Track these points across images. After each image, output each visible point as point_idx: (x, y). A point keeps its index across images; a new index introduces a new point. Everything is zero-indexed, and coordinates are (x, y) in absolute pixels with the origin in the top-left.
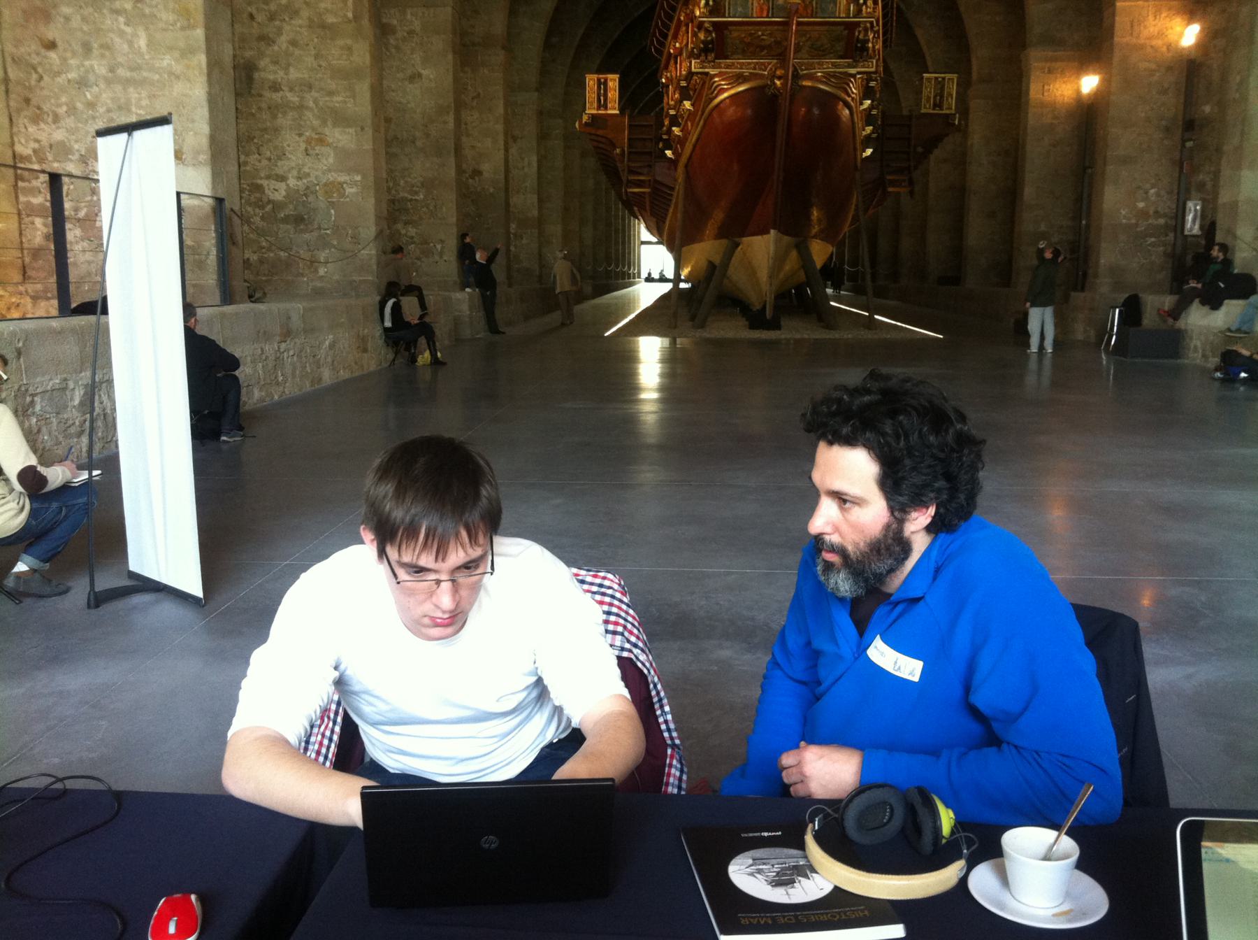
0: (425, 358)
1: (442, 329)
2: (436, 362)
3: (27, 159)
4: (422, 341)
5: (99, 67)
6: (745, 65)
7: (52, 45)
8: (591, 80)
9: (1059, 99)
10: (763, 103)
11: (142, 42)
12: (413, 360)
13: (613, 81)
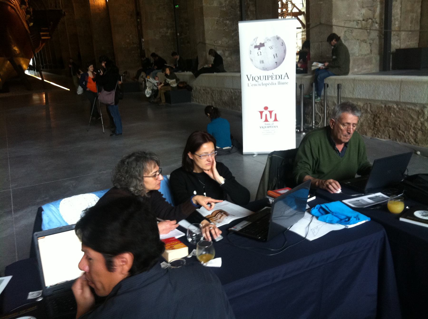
9: (100, 4)
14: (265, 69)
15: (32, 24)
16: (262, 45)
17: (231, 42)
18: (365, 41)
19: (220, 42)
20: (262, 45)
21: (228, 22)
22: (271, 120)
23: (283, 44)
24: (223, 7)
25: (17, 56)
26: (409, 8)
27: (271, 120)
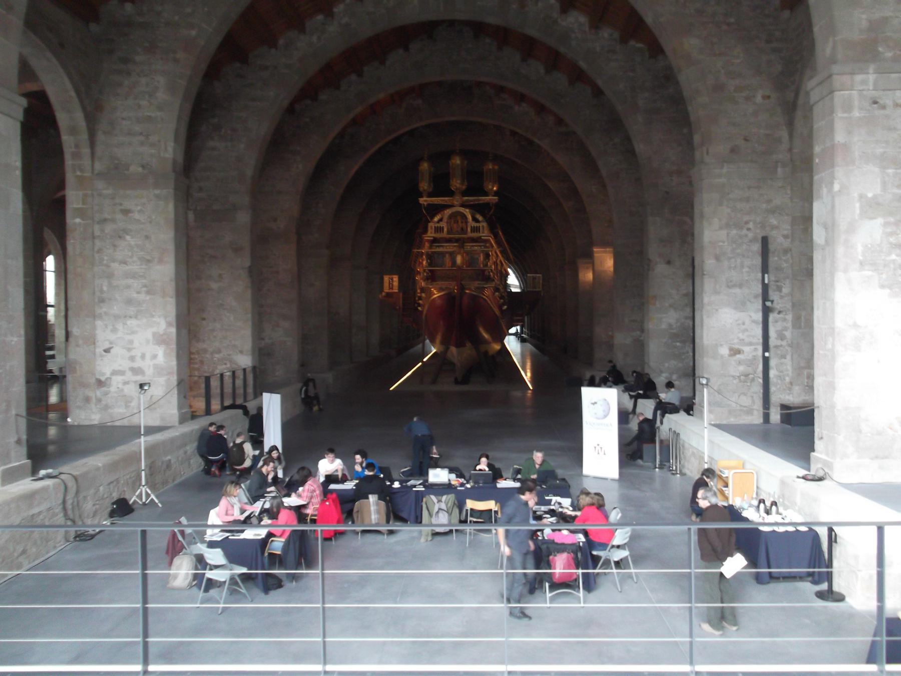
0: (316, 408)
1: (322, 397)
2: (320, 410)
3: (193, 353)
4: (315, 402)
5: (218, 326)
7: (204, 319)
8: (386, 279)
10: (450, 299)
11: (232, 318)
12: (311, 409)
13: (396, 279)
15: (505, 307)
16: (596, 403)
17: (680, 365)
18: (745, 394)
19: (667, 365)
20: (596, 403)
21: (678, 344)
22: (602, 453)
25: (486, 342)
26: (802, 365)
27: (602, 453)
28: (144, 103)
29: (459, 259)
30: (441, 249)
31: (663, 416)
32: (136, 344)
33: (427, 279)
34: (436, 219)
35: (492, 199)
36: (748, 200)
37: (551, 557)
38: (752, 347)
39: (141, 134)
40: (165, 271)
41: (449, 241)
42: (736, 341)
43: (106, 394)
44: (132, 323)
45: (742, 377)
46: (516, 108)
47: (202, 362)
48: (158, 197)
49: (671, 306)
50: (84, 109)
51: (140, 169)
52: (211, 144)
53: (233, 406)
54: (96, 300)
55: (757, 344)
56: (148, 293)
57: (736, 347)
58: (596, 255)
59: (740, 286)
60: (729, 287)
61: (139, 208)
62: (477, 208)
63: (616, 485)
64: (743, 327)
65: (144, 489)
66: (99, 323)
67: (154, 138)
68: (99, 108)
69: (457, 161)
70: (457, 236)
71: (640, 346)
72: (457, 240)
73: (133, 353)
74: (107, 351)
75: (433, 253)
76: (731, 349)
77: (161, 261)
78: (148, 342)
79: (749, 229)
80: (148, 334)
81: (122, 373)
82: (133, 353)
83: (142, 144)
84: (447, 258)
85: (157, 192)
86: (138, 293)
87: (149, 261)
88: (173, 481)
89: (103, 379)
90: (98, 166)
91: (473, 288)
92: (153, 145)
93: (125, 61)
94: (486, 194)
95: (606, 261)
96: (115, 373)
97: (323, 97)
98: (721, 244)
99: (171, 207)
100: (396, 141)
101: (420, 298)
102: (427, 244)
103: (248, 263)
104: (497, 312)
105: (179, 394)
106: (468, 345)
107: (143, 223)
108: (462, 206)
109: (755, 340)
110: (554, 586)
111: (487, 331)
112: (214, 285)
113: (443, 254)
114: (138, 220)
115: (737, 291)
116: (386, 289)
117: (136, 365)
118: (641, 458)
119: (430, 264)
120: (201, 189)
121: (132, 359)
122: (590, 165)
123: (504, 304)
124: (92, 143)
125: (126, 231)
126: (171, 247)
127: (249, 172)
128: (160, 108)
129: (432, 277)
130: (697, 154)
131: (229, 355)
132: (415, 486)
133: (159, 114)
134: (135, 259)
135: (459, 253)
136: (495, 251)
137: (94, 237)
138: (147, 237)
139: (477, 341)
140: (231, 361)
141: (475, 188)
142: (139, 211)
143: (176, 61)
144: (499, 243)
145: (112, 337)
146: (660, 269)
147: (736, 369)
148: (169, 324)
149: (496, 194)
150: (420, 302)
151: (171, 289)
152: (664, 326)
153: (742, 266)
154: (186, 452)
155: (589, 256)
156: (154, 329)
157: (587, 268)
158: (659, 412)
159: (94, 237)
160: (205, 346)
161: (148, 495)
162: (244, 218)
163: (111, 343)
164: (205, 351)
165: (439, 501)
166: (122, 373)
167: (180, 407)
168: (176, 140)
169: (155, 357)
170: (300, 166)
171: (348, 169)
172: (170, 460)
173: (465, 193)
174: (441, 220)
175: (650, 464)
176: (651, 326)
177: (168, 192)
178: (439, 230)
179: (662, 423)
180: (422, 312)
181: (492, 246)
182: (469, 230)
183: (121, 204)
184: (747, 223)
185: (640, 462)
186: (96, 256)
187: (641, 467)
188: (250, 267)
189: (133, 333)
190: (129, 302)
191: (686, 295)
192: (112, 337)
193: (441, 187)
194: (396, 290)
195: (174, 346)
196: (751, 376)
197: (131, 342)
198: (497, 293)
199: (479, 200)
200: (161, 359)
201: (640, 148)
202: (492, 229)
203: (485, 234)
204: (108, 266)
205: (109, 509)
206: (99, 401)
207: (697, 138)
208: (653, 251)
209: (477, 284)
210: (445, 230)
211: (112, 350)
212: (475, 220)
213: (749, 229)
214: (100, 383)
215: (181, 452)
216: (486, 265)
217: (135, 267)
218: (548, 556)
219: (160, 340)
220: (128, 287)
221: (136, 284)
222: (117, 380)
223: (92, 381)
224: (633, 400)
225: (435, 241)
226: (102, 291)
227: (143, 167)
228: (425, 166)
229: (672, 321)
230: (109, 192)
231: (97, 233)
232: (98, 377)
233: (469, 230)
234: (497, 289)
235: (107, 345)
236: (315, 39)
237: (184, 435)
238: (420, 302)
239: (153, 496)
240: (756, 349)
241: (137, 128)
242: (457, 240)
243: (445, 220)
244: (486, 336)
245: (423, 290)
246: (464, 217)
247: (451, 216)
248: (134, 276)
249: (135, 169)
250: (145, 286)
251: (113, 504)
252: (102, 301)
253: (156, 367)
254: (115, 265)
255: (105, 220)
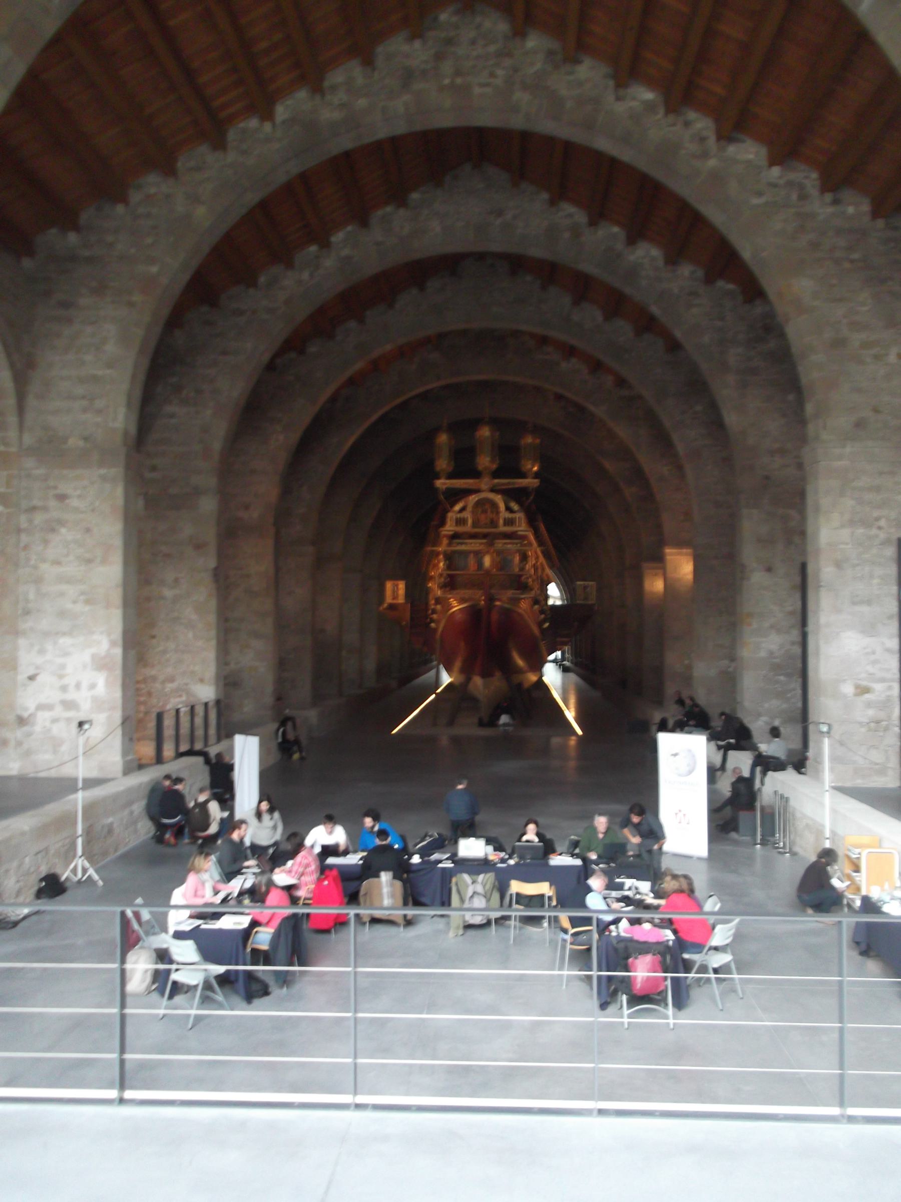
0: (296, 756)
2: (302, 759)
4: (295, 748)
5: (171, 645)
6: (467, 593)
7: (154, 637)
8: (389, 585)
10: (475, 614)
11: (190, 635)
12: (291, 756)
13: (402, 585)
14: (680, 775)
15: (547, 625)
17: (784, 706)
19: (766, 705)
20: (675, 755)
21: (782, 678)
23: (693, 756)
24: (775, 658)
25: (520, 671)
28: (89, 358)
29: (487, 561)
30: (463, 548)
31: (764, 773)
32: (69, 670)
33: (443, 586)
34: (457, 507)
35: (530, 482)
36: (877, 489)
37: (630, 960)
38: (886, 684)
39: (84, 397)
40: (111, 573)
41: (474, 536)
42: (863, 675)
43: (29, 735)
44: (65, 641)
45: (872, 725)
46: (564, 365)
47: (149, 694)
48: (104, 478)
49: (772, 627)
50: (12, 365)
51: (81, 443)
52: (169, 409)
53: (190, 753)
54: (20, 612)
55: (892, 680)
56: (88, 602)
57: (864, 683)
58: (668, 558)
59: (869, 602)
60: (854, 603)
61: (78, 492)
62: (511, 494)
63: (703, 866)
64: (873, 657)
65: (80, 862)
66: (22, 642)
67: (99, 404)
68: (30, 364)
69: (485, 432)
70: (486, 530)
71: (730, 681)
72: (485, 536)
73: (66, 681)
74: (32, 678)
75: (454, 552)
76: (857, 687)
77: (104, 561)
78: (85, 667)
79: (880, 528)
80: (86, 656)
81: (48, 707)
82: (66, 681)
83: (85, 410)
84: (472, 561)
85: (103, 471)
86: (75, 602)
87: (89, 561)
88: (116, 851)
89: (25, 715)
90: (28, 439)
91: (504, 598)
92: (99, 412)
93: (66, 305)
94: (523, 476)
95: (683, 566)
96: (41, 707)
97: (312, 349)
98: (842, 546)
99: (119, 491)
100: (404, 405)
101: (434, 612)
102: (445, 541)
103: (212, 563)
104: (536, 630)
105: (124, 735)
106: (498, 674)
107: (82, 512)
108: (493, 490)
109: (888, 676)
110: (636, 999)
111: (523, 655)
112: (168, 593)
113: (465, 554)
114: (77, 510)
115: (865, 609)
116: (389, 600)
117: (69, 696)
118: (736, 829)
119: (449, 567)
120: (154, 469)
121: (64, 689)
122: (662, 441)
123: (544, 621)
124: (21, 409)
125: (62, 523)
126: (118, 542)
127: (217, 446)
128: (109, 365)
129: (451, 584)
130: (811, 428)
131: (186, 684)
132: (440, 862)
133: (108, 372)
134: (71, 558)
135: (488, 552)
136: (535, 552)
137: (19, 531)
138: (88, 530)
139: (508, 669)
140: (189, 693)
141: (508, 468)
142: (79, 496)
143: (131, 304)
144: (541, 543)
145: (39, 660)
146: (757, 578)
147: (863, 713)
148: (113, 644)
149: (537, 475)
150: (435, 616)
151: (116, 596)
152: (763, 654)
153: (871, 577)
154: (132, 813)
155: (658, 559)
156: (93, 650)
157: (656, 575)
158: (758, 769)
159: (19, 531)
160: (153, 672)
161: (85, 871)
162: (208, 505)
163: (37, 667)
164: (154, 679)
165: (474, 882)
166: (48, 707)
167: (125, 753)
168: (129, 405)
169: (93, 686)
170: (281, 437)
171: (343, 442)
172: (112, 824)
173: (496, 474)
174: (463, 509)
175: (747, 839)
176: (745, 653)
177: (117, 471)
178: (461, 522)
179: (762, 783)
180: (435, 630)
181: (530, 544)
182: (501, 522)
183: (55, 488)
184: (877, 519)
185: (734, 835)
186: (22, 554)
187: (736, 842)
188: (216, 569)
189: (66, 654)
190: (62, 614)
191: (792, 613)
192: (39, 660)
193: (464, 467)
194: (401, 600)
195: (118, 672)
196: (884, 723)
197: (63, 667)
198: (536, 607)
199: (513, 483)
200: (101, 688)
201: (731, 419)
202: (531, 522)
203: (522, 527)
204: (35, 567)
205: (36, 888)
206: (19, 744)
207: (809, 408)
208: (749, 553)
209: (510, 593)
210: (470, 522)
211: (39, 678)
212: (509, 509)
213: (880, 528)
214: (22, 721)
215: (126, 812)
216: (522, 569)
217: (71, 569)
218: (627, 958)
219: (100, 664)
220: (62, 594)
221: (71, 590)
222: (43, 718)
223: (11, 718)
224: (722, 751)
225: (455, 536)
226: (27, 601)
227: (86, 439)
228: (443, 438)
229: (774, 647)
230: (41, 471)
231: (24, 525)
232: (19, 712)
233: (501, 522)
234: (536, 602)
235: (31, 672)
236: (305, 275)
237: (129, 791)
238: (435, 616)
239: (91, 872)
240: (890, 688)
241: (80, 390)
242: (485, 536)
243: (469, 508)
244: (520, 662)
245: (438, 601)
246: (494, 505)
247: (478, 504)
248: (69, 581)
249: (74, 442)
250: (82, 593)
251: (41, 880)
252: (27, 612)
253: (95, 699)
254: (44, 567)
255: (33, 509)
